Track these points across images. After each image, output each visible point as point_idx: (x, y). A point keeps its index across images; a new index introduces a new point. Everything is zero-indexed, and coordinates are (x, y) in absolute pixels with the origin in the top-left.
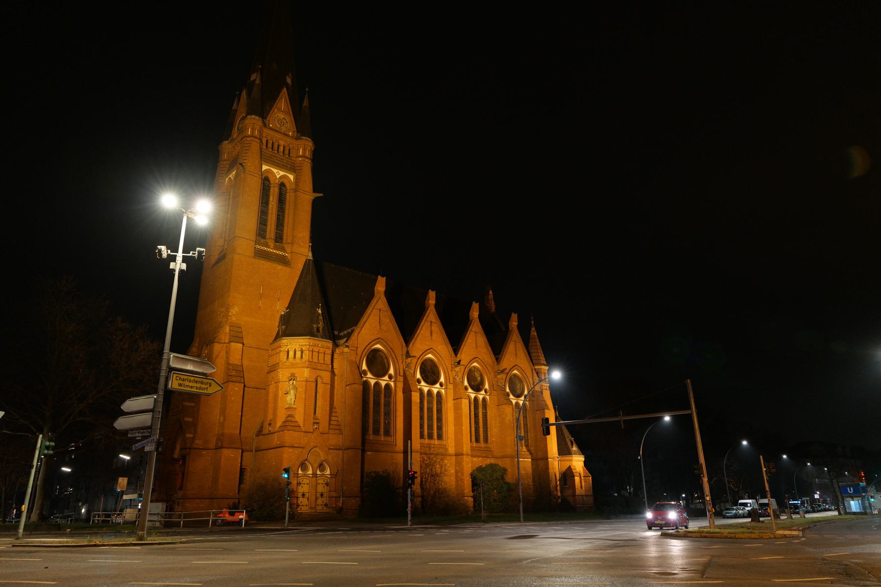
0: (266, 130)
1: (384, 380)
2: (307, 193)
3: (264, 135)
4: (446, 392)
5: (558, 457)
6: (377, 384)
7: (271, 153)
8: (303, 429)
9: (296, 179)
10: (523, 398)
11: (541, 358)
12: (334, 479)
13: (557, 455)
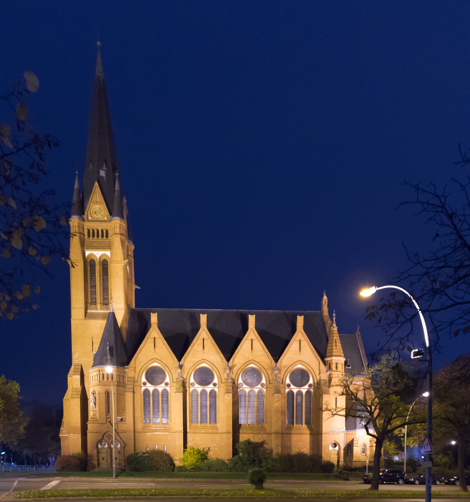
0: (87, 225)
1: (161, 387)
2: (119, 262)
3: (85, 228)
4: (218, 389)
5: (344, 432)
6: (155, 391)
7: (92, 240)
8: (99, 422)
9: (111, 254)
10: (307, 387)
11: (334, 350)
12: (123, 450)
13: (344, 430)
